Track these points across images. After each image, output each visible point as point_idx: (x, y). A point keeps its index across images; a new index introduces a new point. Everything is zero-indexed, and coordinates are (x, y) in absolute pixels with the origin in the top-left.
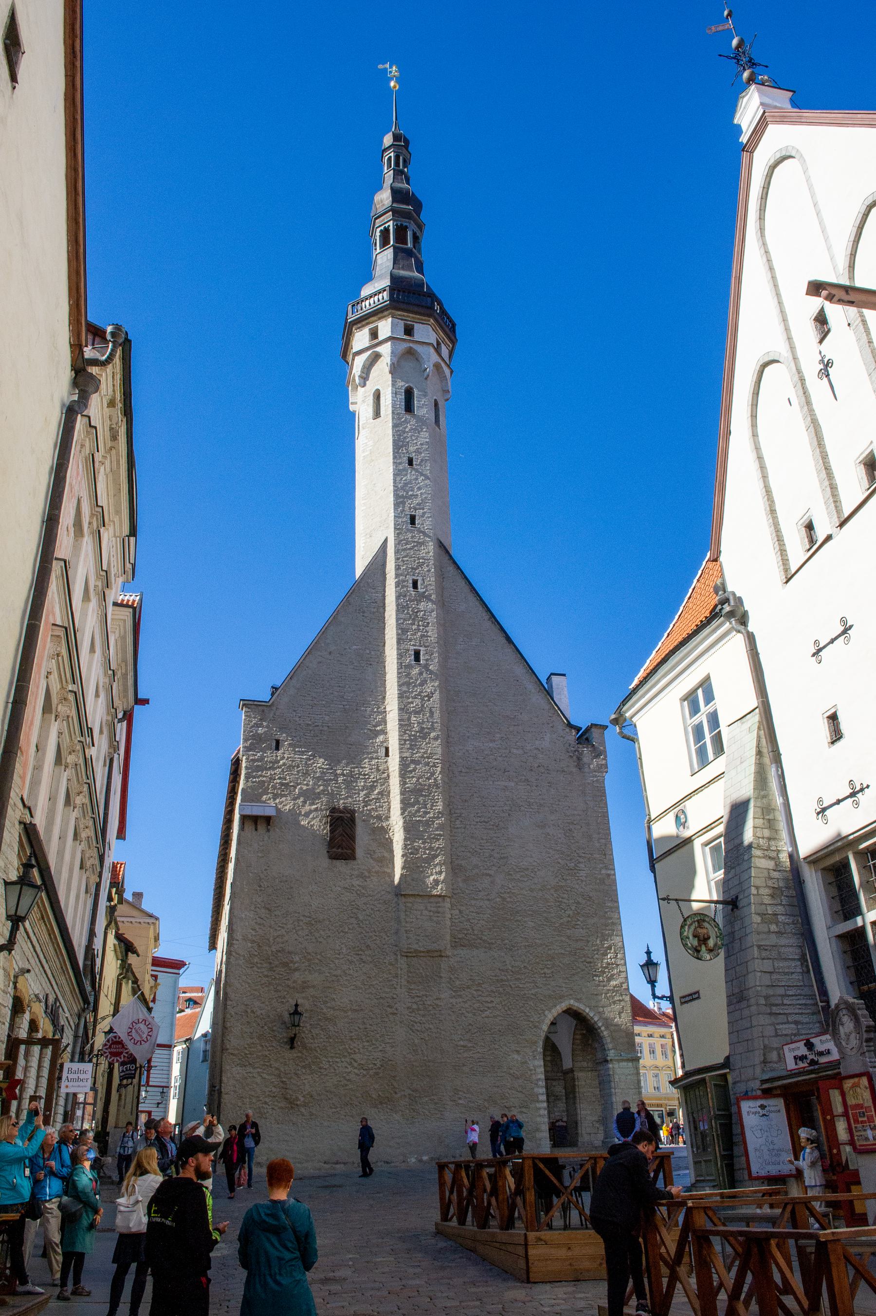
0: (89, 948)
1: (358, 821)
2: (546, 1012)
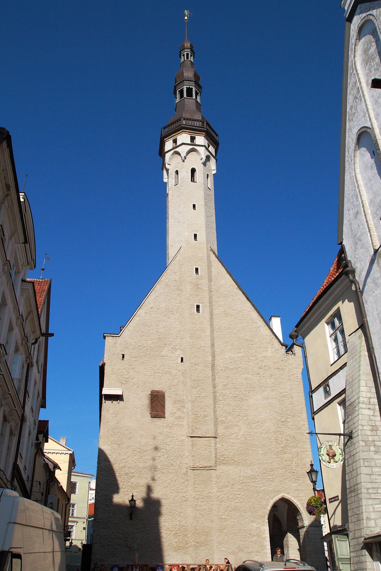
2: (270, 500)
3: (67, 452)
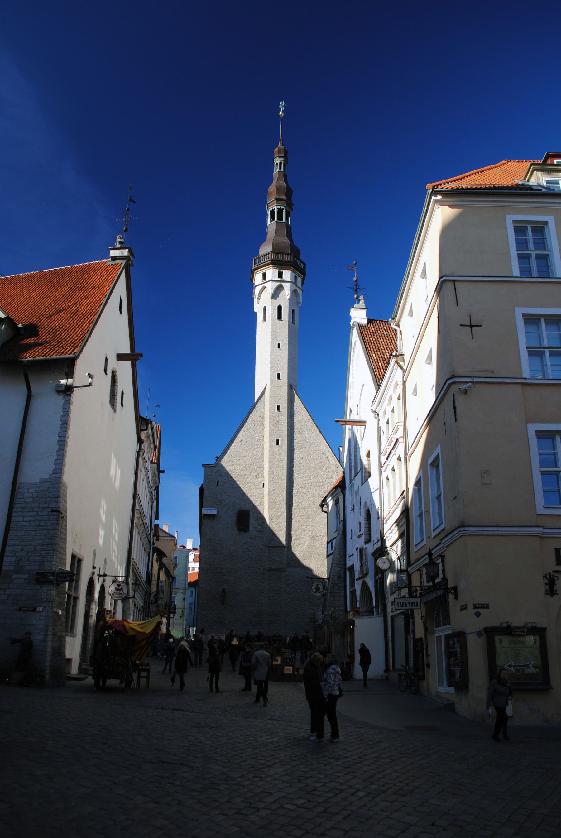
1: (251, 516)
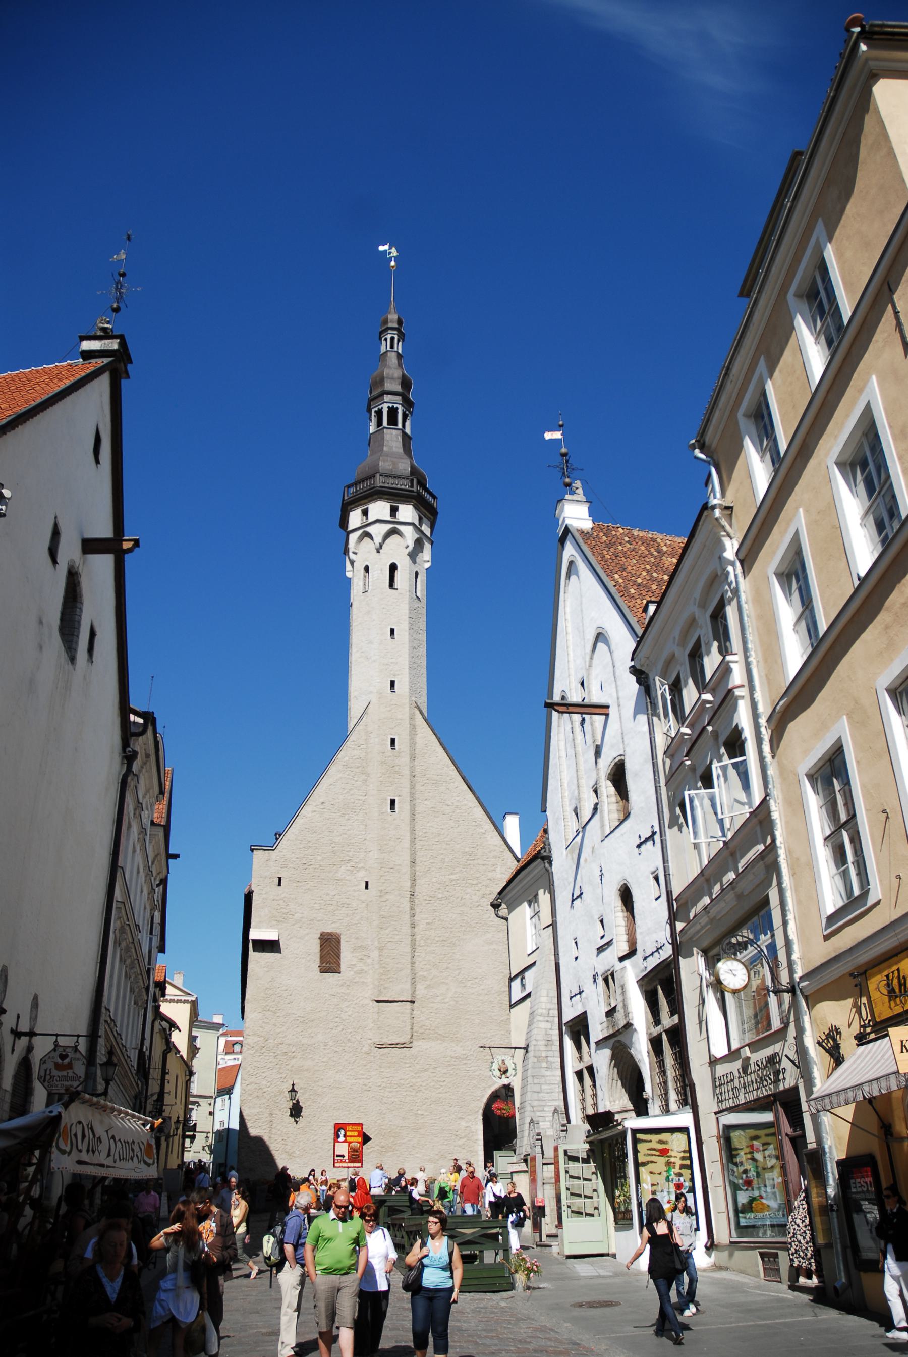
0: (141, 1054)
3: (186, 998)
